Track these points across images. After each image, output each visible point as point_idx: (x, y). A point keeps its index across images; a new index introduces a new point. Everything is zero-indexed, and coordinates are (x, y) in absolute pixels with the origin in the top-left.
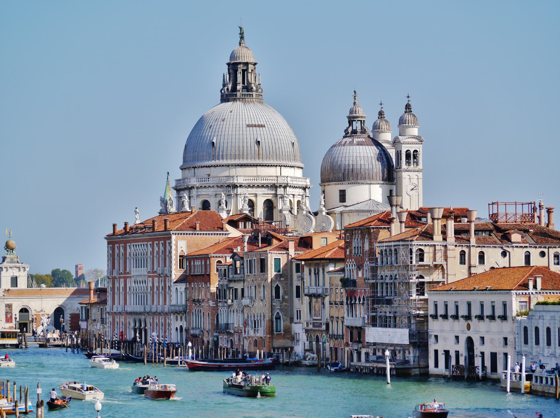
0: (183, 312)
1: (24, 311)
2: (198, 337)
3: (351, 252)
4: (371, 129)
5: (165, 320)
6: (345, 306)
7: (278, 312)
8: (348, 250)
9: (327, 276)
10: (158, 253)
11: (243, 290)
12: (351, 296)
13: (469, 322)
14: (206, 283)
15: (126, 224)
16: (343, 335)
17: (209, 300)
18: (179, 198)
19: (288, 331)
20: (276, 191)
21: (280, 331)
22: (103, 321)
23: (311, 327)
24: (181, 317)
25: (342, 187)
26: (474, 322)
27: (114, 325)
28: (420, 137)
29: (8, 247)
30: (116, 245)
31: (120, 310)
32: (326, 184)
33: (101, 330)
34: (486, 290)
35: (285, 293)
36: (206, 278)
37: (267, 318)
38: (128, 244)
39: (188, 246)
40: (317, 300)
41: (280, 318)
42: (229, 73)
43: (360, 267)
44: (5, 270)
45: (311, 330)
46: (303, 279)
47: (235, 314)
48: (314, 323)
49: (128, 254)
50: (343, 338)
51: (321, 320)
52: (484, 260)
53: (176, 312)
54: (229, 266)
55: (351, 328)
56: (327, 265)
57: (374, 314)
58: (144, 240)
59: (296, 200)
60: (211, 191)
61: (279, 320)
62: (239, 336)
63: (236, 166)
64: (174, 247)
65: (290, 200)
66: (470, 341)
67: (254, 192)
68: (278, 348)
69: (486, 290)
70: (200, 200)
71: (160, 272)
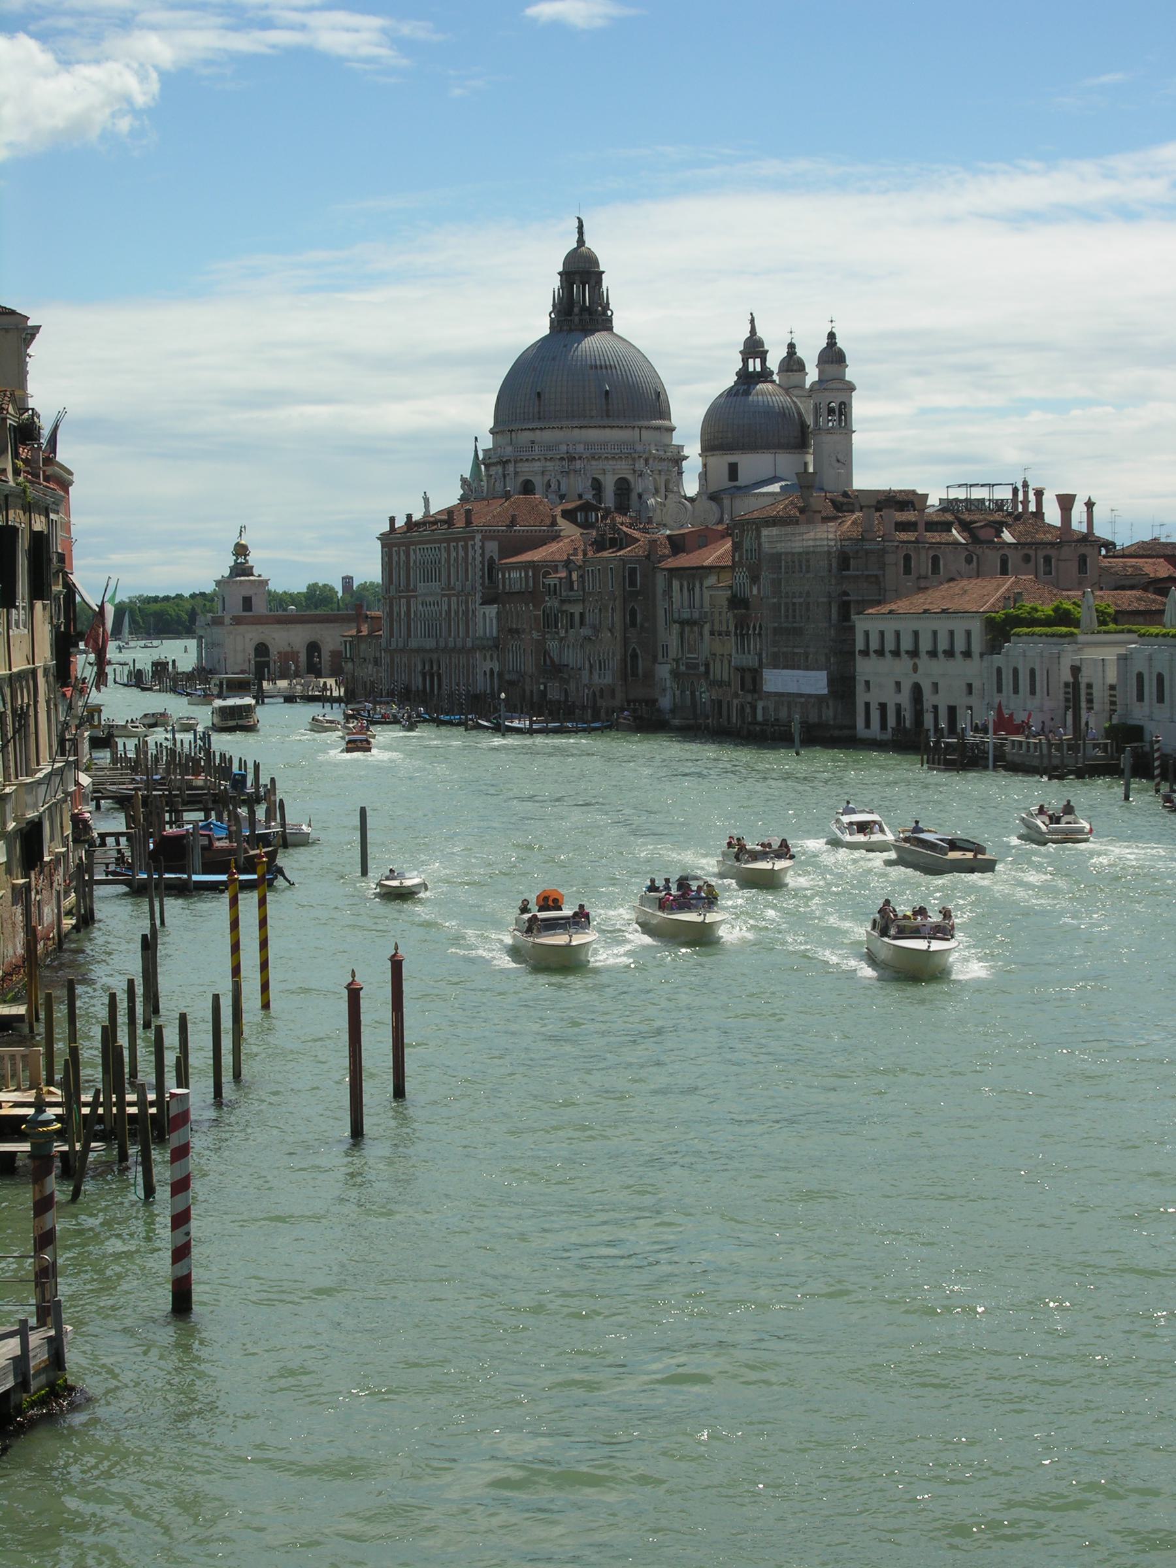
1: (262, 649)
3: (741, 557)
4: (776, 370)
6: (733, 639)
7: (634, 649)
8: (737, 555)
9: (707, 594)
10: (456, 559)
13: (916, 660)
14: (527, 605)
15: (409, 517)
16: (729, 682)
19: (649, 675)
22: (377, 662)
24: (491, 655)
25: (732, 458)
26: (924, 661)
28: (850, 382)
30: (395, 549)
32: (708, 454)
33: (375, 675)
34: (941, 613)
37: (619, 658)
43: (755, 579)
46: (672, 597)
48: (687, 663)
49: (412, 561)
50: (730, 685)
51: (697, 659)
52: (939, 568)
55: (742, 670)
57: (776, 649)
58: (435, 542)
59: (663, 478)
60: (537, 466)
63: (572, 427)
66: (917, 690)
68: (635, 701)
69: (941, 613)
70: (521, 479)
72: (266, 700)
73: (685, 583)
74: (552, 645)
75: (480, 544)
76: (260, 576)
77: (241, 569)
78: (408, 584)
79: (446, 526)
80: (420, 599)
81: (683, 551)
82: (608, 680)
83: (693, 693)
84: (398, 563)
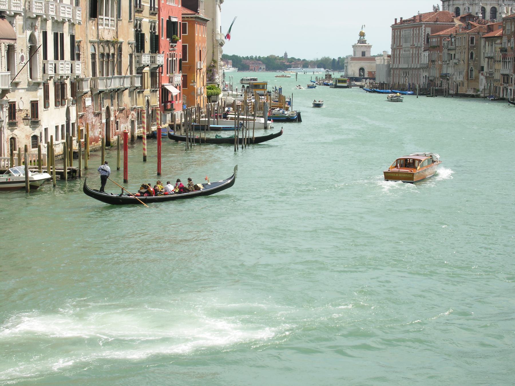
1: (362, 69)
2: (433, 81)
3: (505, 32)
6: (501, 63)
8: (504, 31)
10: (416, 34)
11: (455, 54)
12: (504, 57)
15: (401, 18)
16: (500, 80)
18: (443, 6)
19: (477, 78)
20: (498, 2)
21: (472, 78)
23: (488, 75)
30: (396, 30)
31: (396, 67)
35: (476, 56)
37: (465, 71)
39: (433, 31)
40: (491, 60)
41: (473, 70)
43: (509, 41)
45: (488, 77)
47: (450, 68)
50: (500, 81)
53: (423, 68)
54: (448, 41)
55: (504, 75)
56: (497, 40)
61: (472, 72)
62: (452, 80)
65: (506, 8)
67: (485, 2)
70: (455, 7)
71: (416, 45)
72: (352, 87)
73: (490, 43)
74: (445, 66)
75: (424, 28)
76: (368, 44)
77: (362, 41)
78: (400, 44)
79: (413, 22)
81: (492, 31)
82: (461, 79)
83: (491, 84)
84: (397, 36)
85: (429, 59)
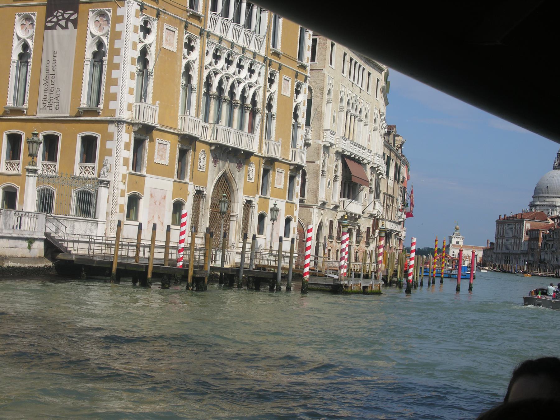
0: (525, 254)
5: (518, 257)
10: (517, 228)
11: (552, 245)
14: (537, 241)
17: (537, 249)
18: (531, 210)
22: (492, 256)
27: (496, 258)
29: (457, 229)
31: (499, 252)
36: (537, 239)
38: (505, 224)
39: (531, 226)
42: (558, 158)
44: (454, 238)
60: (545, 208)
64: (524, 226)
80: (506, 240)
84: (501, 228)
85: (528, 247)
